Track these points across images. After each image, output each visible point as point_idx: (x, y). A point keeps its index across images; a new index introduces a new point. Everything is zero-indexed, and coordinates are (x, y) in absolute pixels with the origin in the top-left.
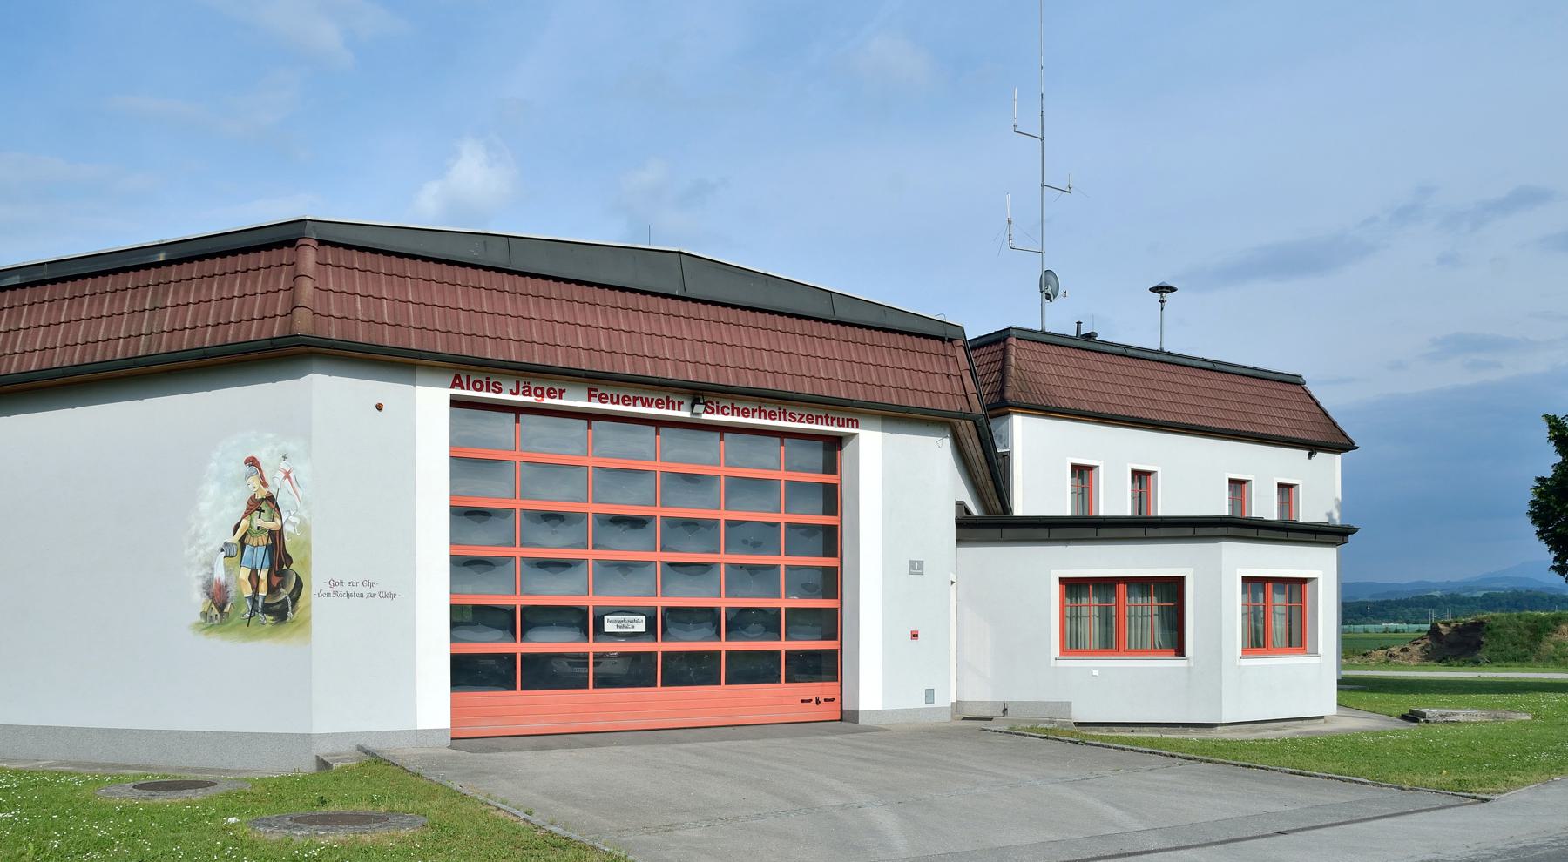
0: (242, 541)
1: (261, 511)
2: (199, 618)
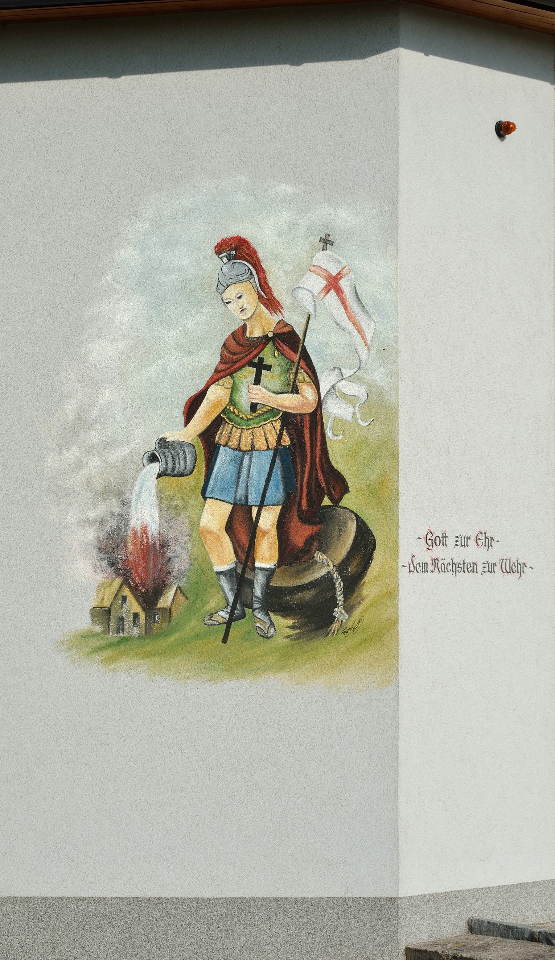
0: (209, 440)
1: (261, 367)
2: (84, 622)
